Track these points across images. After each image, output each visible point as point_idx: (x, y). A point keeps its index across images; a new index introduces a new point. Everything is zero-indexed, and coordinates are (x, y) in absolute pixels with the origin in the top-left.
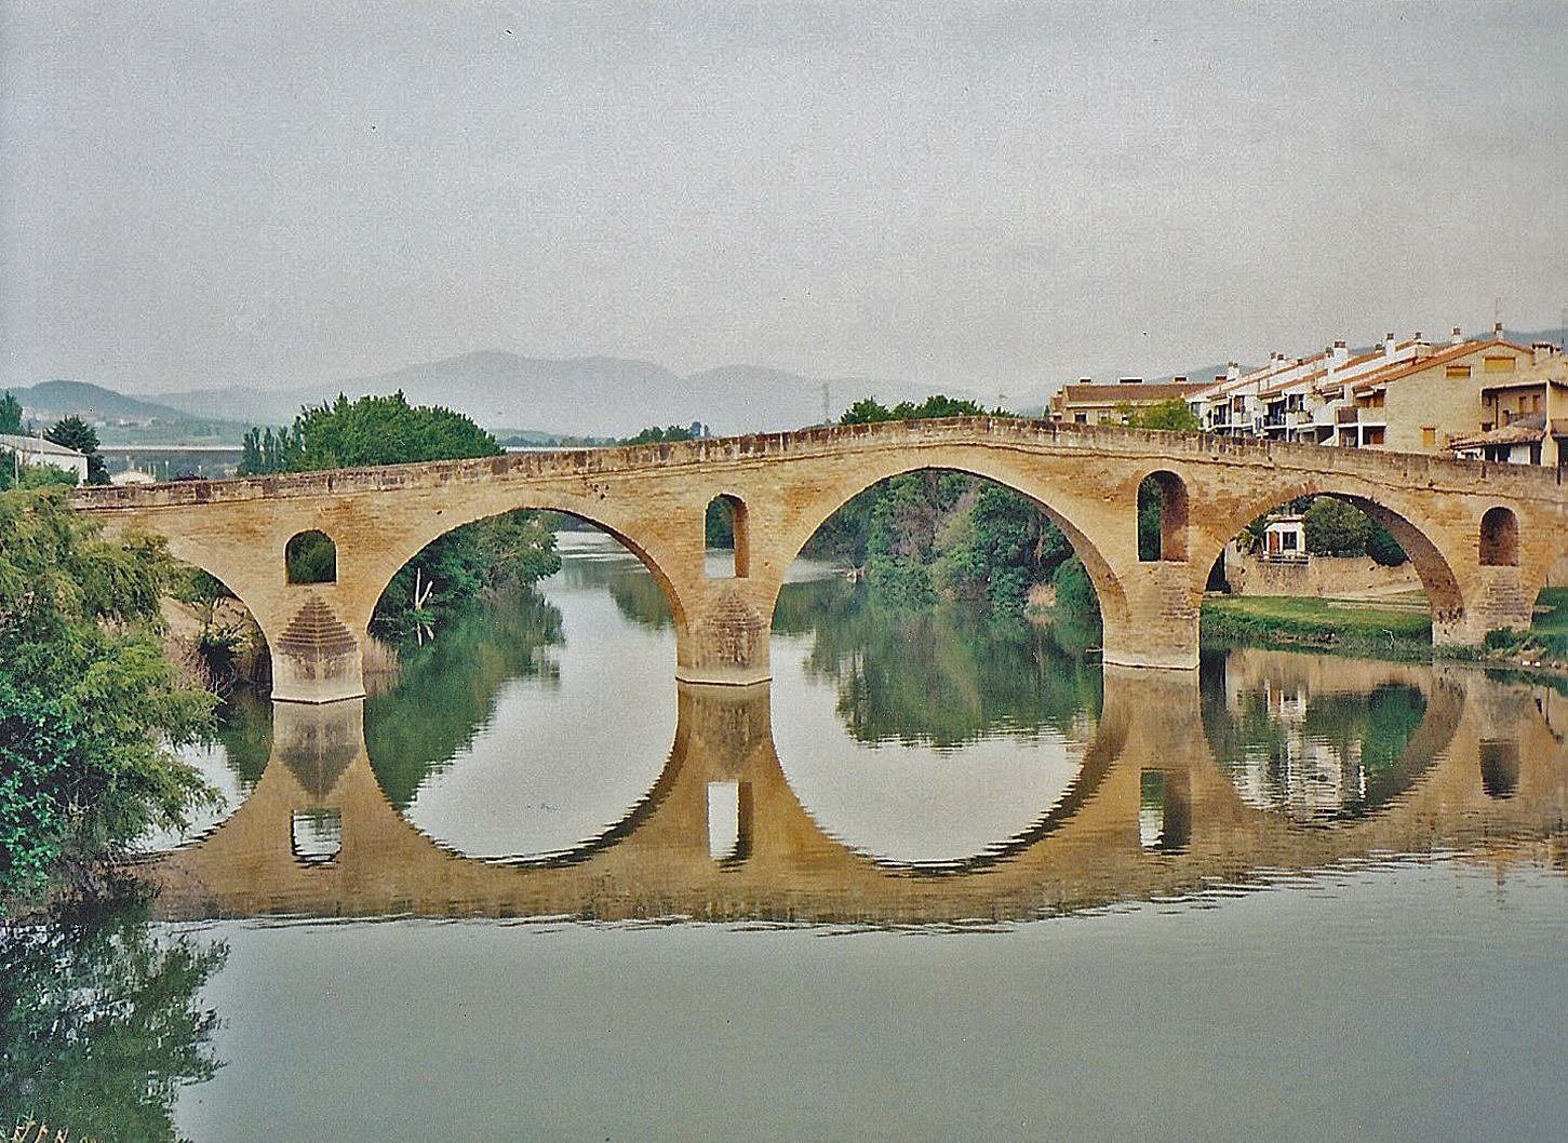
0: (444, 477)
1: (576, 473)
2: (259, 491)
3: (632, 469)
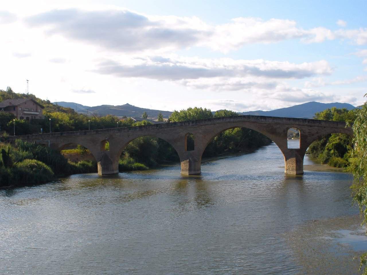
0: (130, 129)
1: (156, 128)
2: (95, 133)
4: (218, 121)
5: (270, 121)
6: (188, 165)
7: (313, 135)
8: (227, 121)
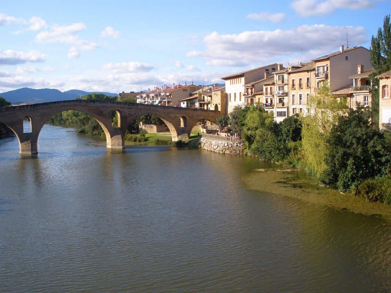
3: (8, 111)
4: (53, 105)
5: (98, 104)
6: (30, 145)
7: (132, 116)
8: (62, 104)
